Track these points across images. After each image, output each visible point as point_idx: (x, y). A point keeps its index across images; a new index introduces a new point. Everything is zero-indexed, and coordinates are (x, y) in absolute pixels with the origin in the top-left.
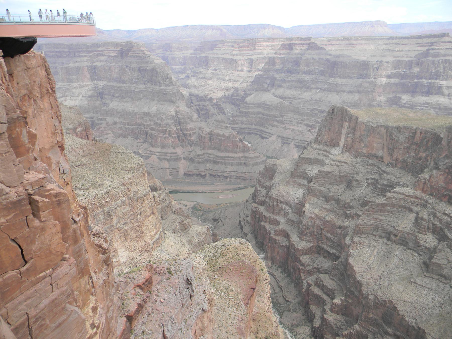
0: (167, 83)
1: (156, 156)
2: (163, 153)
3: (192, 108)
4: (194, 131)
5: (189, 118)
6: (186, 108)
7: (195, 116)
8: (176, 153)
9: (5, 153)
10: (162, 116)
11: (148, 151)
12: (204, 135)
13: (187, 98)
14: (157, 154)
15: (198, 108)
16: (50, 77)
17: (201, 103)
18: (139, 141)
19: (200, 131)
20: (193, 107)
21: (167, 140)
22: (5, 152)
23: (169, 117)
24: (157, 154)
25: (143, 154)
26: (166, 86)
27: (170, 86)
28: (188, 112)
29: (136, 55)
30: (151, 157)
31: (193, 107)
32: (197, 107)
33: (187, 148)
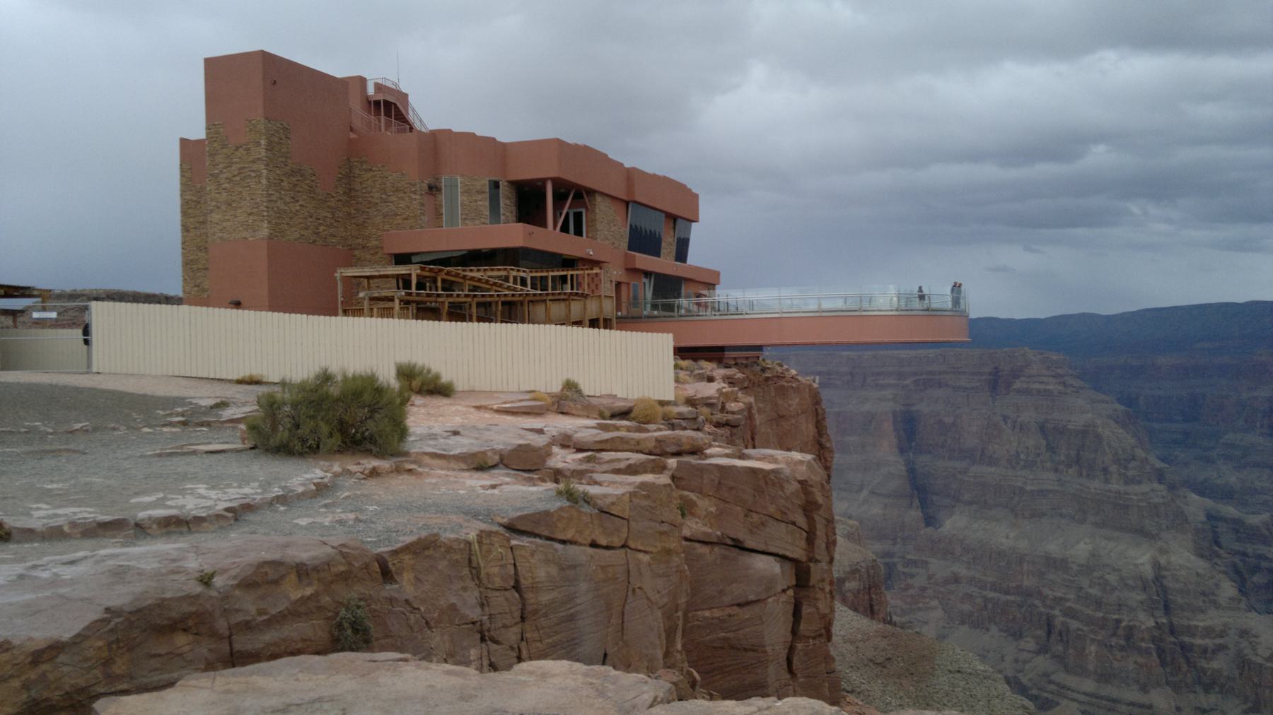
0: (1130, 473)
1: (1075, 705)
2: (1101, 698)
3: (1217, 560)
4: (1218, 641)
5: (1203, 594)
6: (1193, 558)
7: (1228, 589)
8: (1150, 707)
9: (814, 638)
10: (1107, 577)
11: (1050, 682)
12: (1259, 660)
13: (1200, 526)
14: (1082, 698)
15: (1240, 564)
16: (823, 440)
17: (1249, 549)
18: (1022, 644)
19: (1244, 644)
20: (1218, 556)
21: (1119, 657)
22: (813, 635)
23: (1130, 582)
24: (1082, 698)
25: (1034, 692)
26: (1126, 483)
27: (1140, 482)
28: (1201, 571)
29: (1037, 386)
30: (1058, 704)
31: (1218, 556)
32: (1237, 559)
33: (1192, 696)
